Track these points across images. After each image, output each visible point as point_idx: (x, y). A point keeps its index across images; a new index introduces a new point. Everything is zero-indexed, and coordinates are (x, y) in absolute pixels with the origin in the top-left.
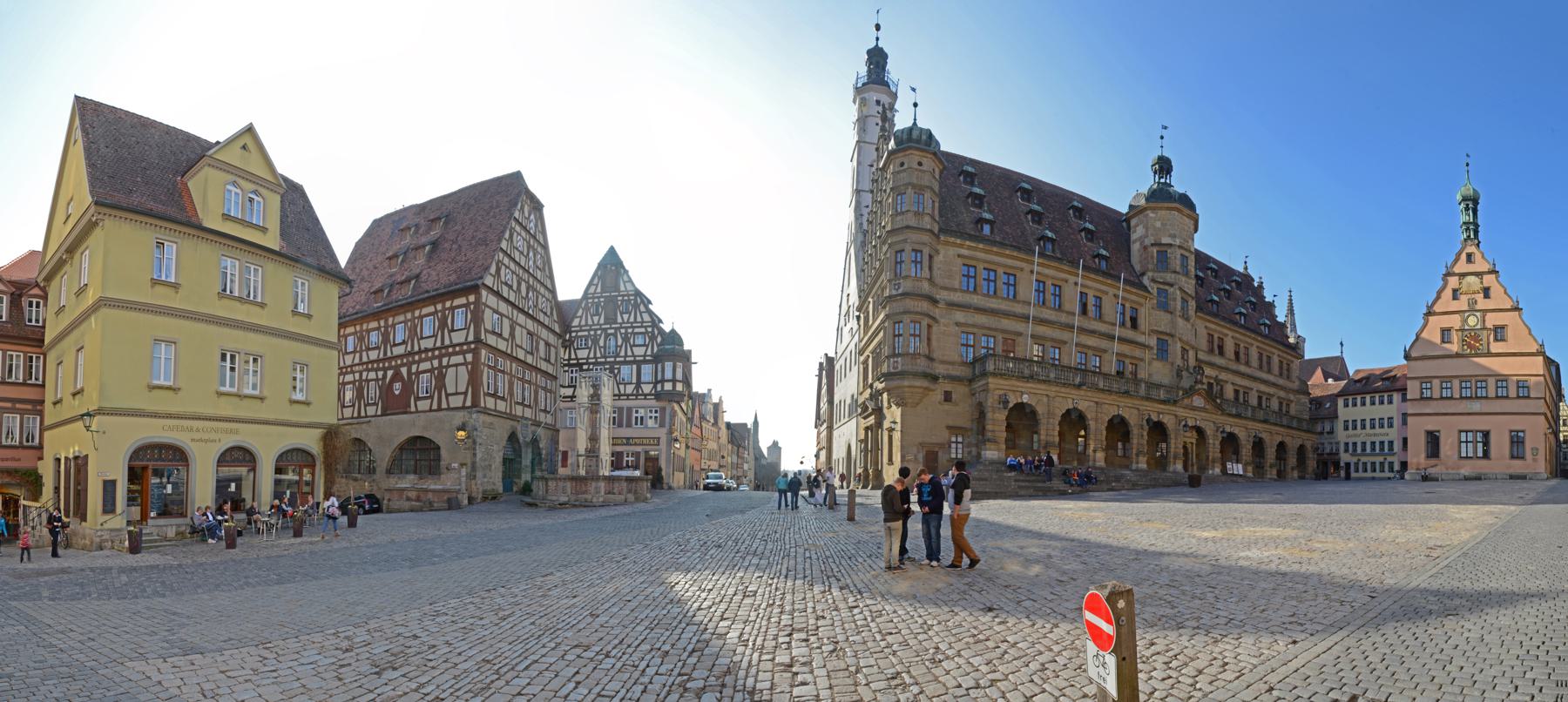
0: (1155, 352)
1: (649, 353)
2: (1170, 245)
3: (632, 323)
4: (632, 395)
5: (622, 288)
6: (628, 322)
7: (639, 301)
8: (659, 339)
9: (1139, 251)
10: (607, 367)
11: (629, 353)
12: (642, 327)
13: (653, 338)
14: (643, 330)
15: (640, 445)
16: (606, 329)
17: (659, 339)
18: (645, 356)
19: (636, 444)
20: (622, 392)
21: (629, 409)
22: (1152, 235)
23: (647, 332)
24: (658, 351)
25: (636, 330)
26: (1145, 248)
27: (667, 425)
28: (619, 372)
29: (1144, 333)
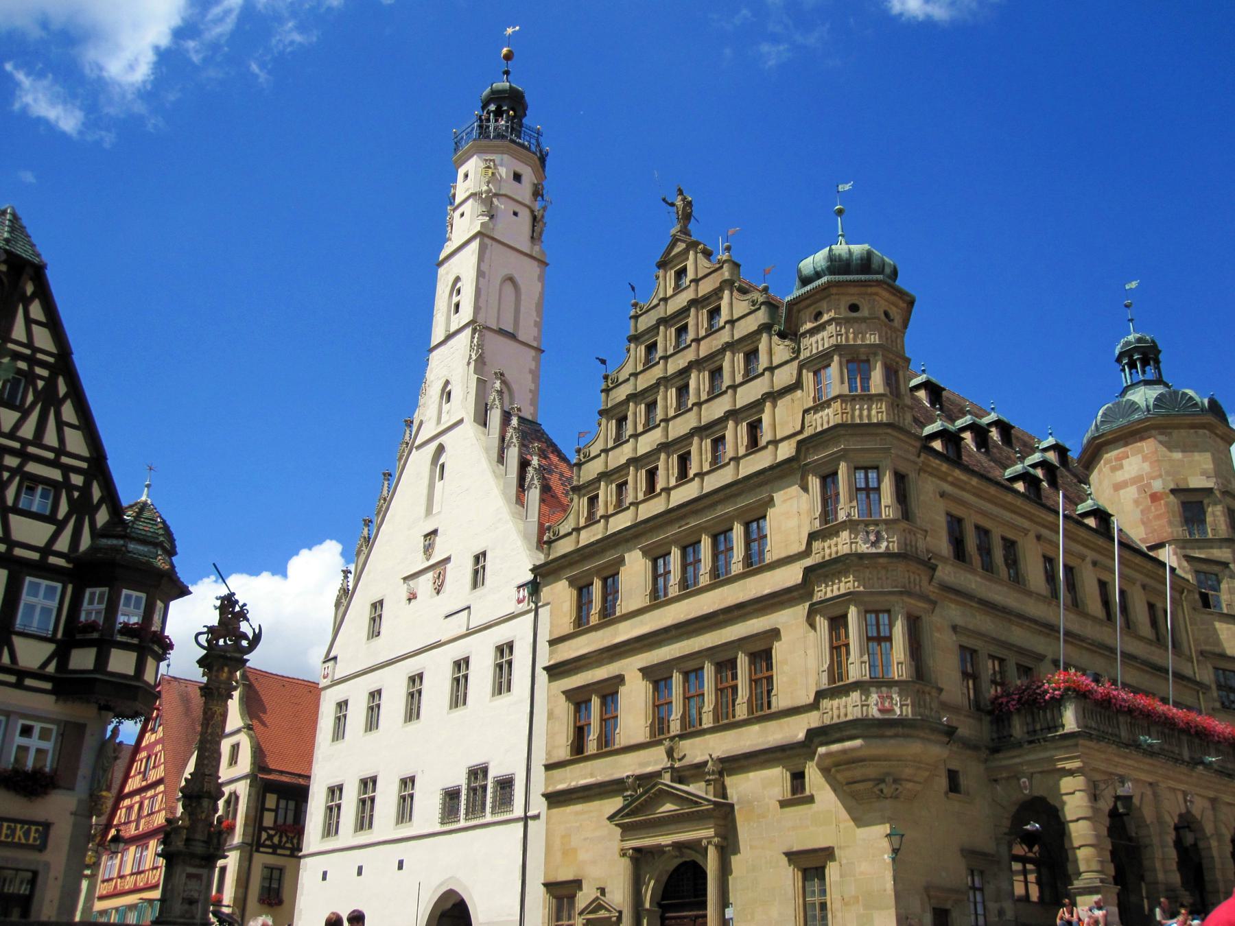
1: (63, 544)
2: (1208, 491)
3: (25, 442)
5: (19, 332)
6: (12, 435)
7: (62, 389)
8: (102, 517)
9: (1137, 502)
13: (82, 507)
14: (56, 475)
17: (102, 517)
18: (47, 550)
22: (1168, 473)
23: (67, 484)
24: (93, 549)
25: (32, 468)
26: (1155, 497)
27: (82, 786)
29: (1190, 660)
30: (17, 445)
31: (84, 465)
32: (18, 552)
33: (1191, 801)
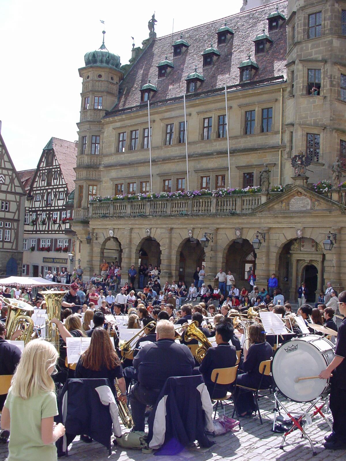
0: (288, 150)
3: (58, 185)
4: (57, 231)
5: (54, 164)
6: (56, 185)
10: (48, 213)
11: (56, 205)
12: (62, 188)
14: (62, 190)
15: (58, 263)
16: (47, 190)
19: (56, 263)
20: (53, 229)
21: (56, 240)
25: (60, 190)
28: (52, 216)
29: (277, 133)
30: (57, 187)
31: (65, 186)
32: (60, 208)
33: (148, 232)
